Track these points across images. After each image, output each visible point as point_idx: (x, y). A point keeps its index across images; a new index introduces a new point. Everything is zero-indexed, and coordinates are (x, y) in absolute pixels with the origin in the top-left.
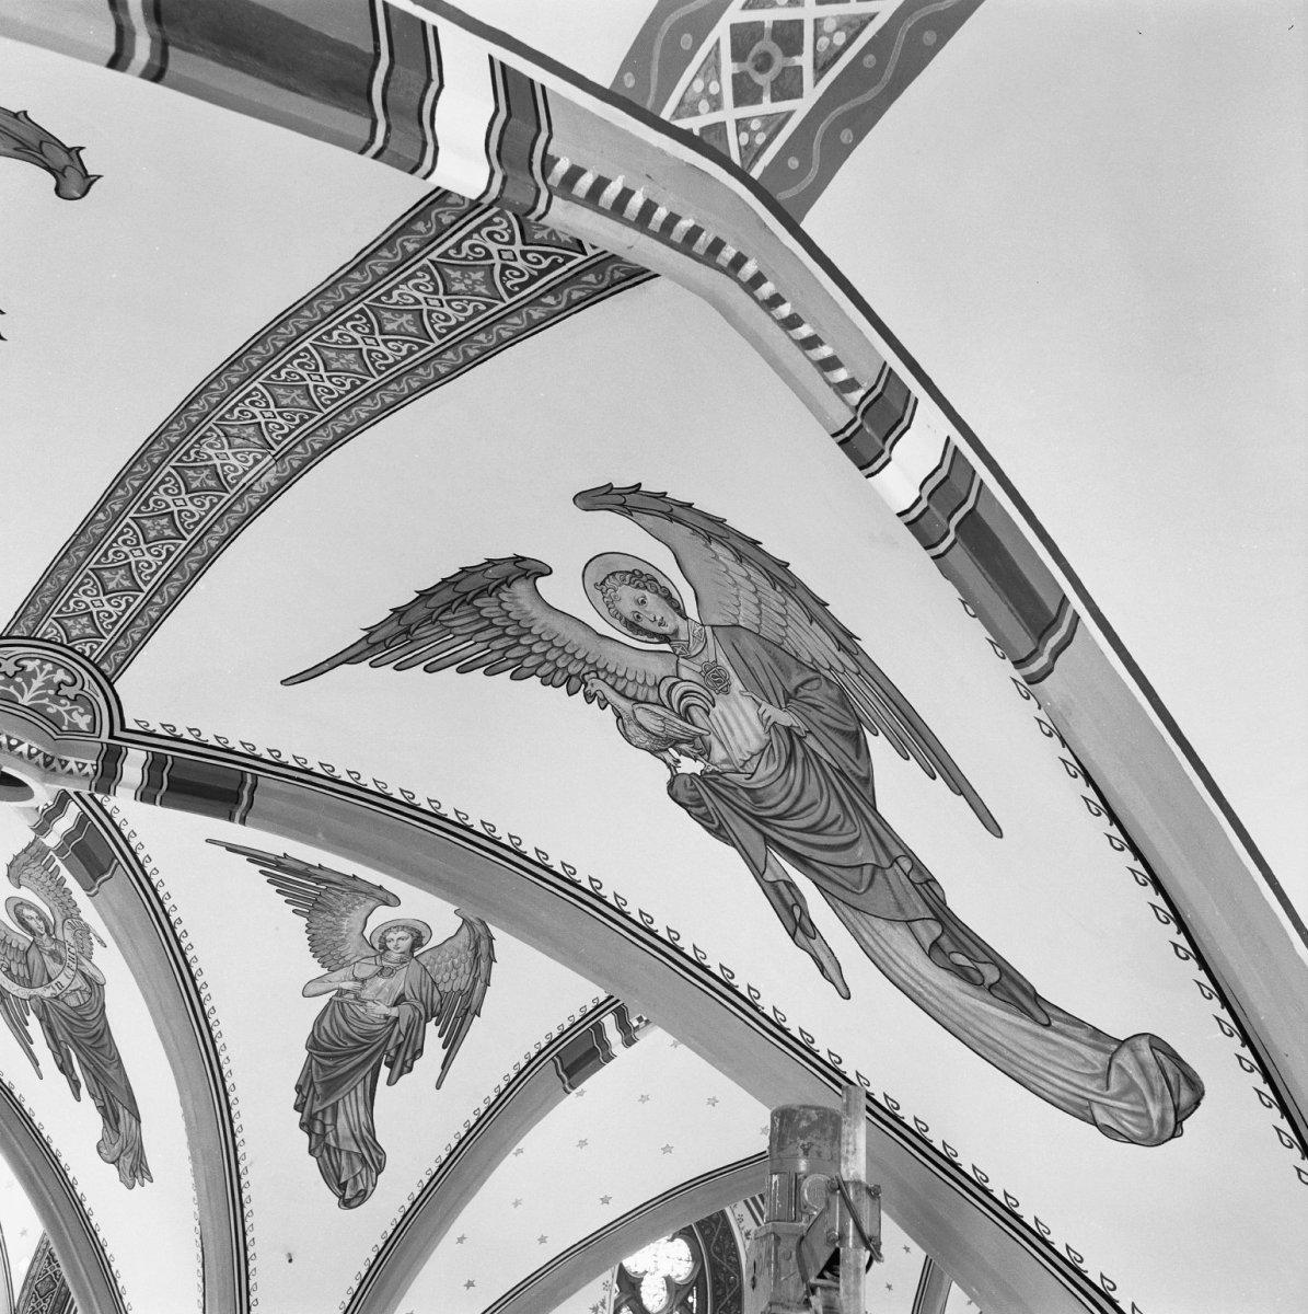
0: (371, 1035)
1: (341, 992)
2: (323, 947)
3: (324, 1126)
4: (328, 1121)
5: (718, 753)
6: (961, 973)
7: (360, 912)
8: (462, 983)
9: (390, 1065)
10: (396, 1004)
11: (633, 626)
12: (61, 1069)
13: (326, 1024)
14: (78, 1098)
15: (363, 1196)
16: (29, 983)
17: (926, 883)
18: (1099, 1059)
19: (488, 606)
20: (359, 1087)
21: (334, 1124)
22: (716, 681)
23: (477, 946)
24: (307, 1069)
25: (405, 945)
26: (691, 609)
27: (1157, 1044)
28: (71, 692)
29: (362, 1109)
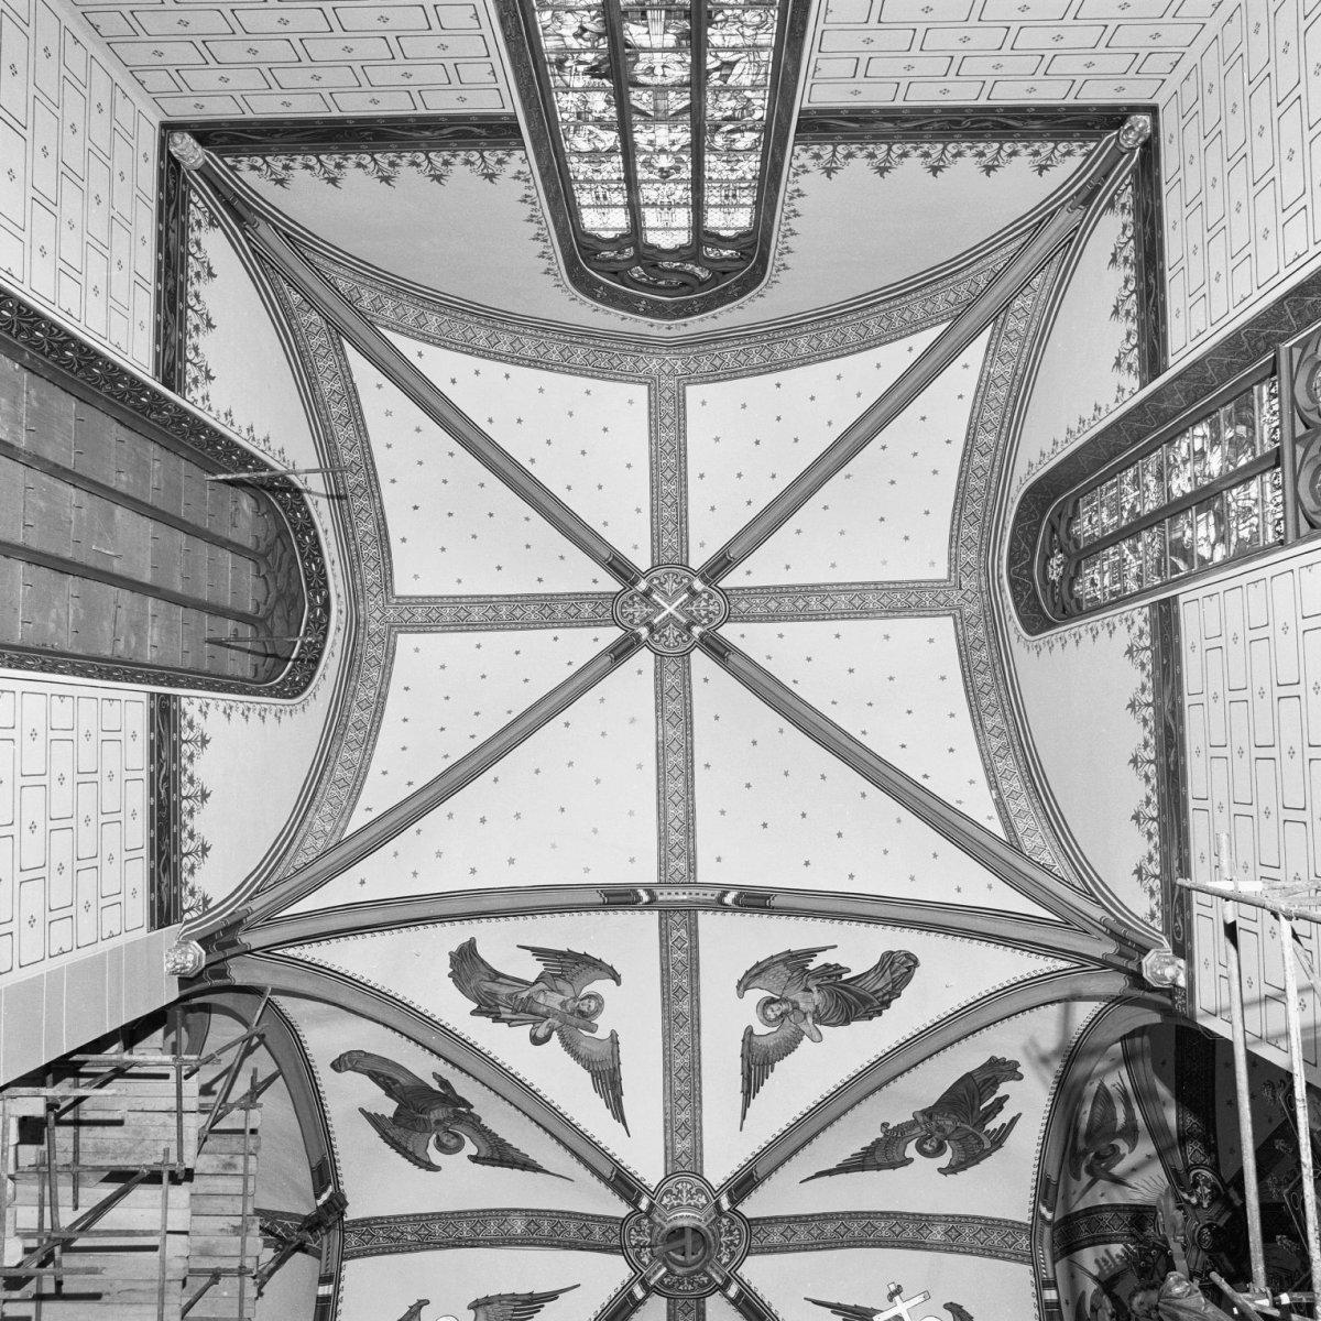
0: (830, 994)
1: (816, 1021)
2: (789, 1046)
3: (885, 995)
4: (880, 994)
5: (450, 1110)
6: (389, 1078)
7: (763, 1041)
8: (781, 967)
9: (840, 976)
10: (810, 991)
11: (457, 1136)
12: (1001, 1108)
13: (832, 1021)
14: (1007, 1097)
15: (908, 955)
16: (976, 1137)
17: (390, 1093)
18: (359, 1066)
19: (497, 1156)
20: (860, 985)
21: (881, 989)
22: (438, 1122)
23: (756, 975)
24: (858, 1019)
25: (774, 1007)
26: (434, 1136)
27: (336, 1070)
28: (637, 1228)
29: (868, 979)
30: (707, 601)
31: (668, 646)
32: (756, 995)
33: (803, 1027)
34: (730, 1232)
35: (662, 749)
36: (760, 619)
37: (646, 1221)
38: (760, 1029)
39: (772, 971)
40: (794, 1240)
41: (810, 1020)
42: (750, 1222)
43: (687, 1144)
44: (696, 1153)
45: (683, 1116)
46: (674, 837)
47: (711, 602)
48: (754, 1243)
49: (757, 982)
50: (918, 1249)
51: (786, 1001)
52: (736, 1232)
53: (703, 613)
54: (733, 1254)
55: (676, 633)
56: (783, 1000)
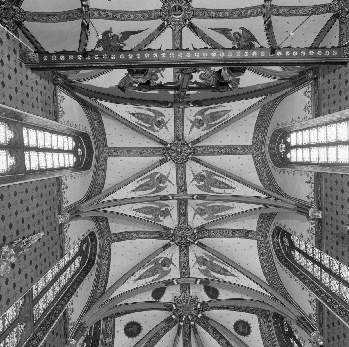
8: (250, 36)
25: (238, 36)
30: (345, 17)
31: (333, 7)
32: (241, 32)
33: (235, 42)
34: (179, 25)
35: (303, 8)
36: (340, 32)
37: (182, 2)
38: (232, 33)
39: (248, 34)
40: (176, 43)
41: (237, 43)
42: (181, 31)
43: (200, 15)
44: (198, 17)
45: (207, 14)
46: (281, 11)
47: (345, 18)
48: (175, 32)
49: (244, 32)
50: (174, 76)
51: (241, 38)
52: (178, 27)
53: (342, 16)
54: (173, 26)
55: (337, 9)
56: (241, 38)
